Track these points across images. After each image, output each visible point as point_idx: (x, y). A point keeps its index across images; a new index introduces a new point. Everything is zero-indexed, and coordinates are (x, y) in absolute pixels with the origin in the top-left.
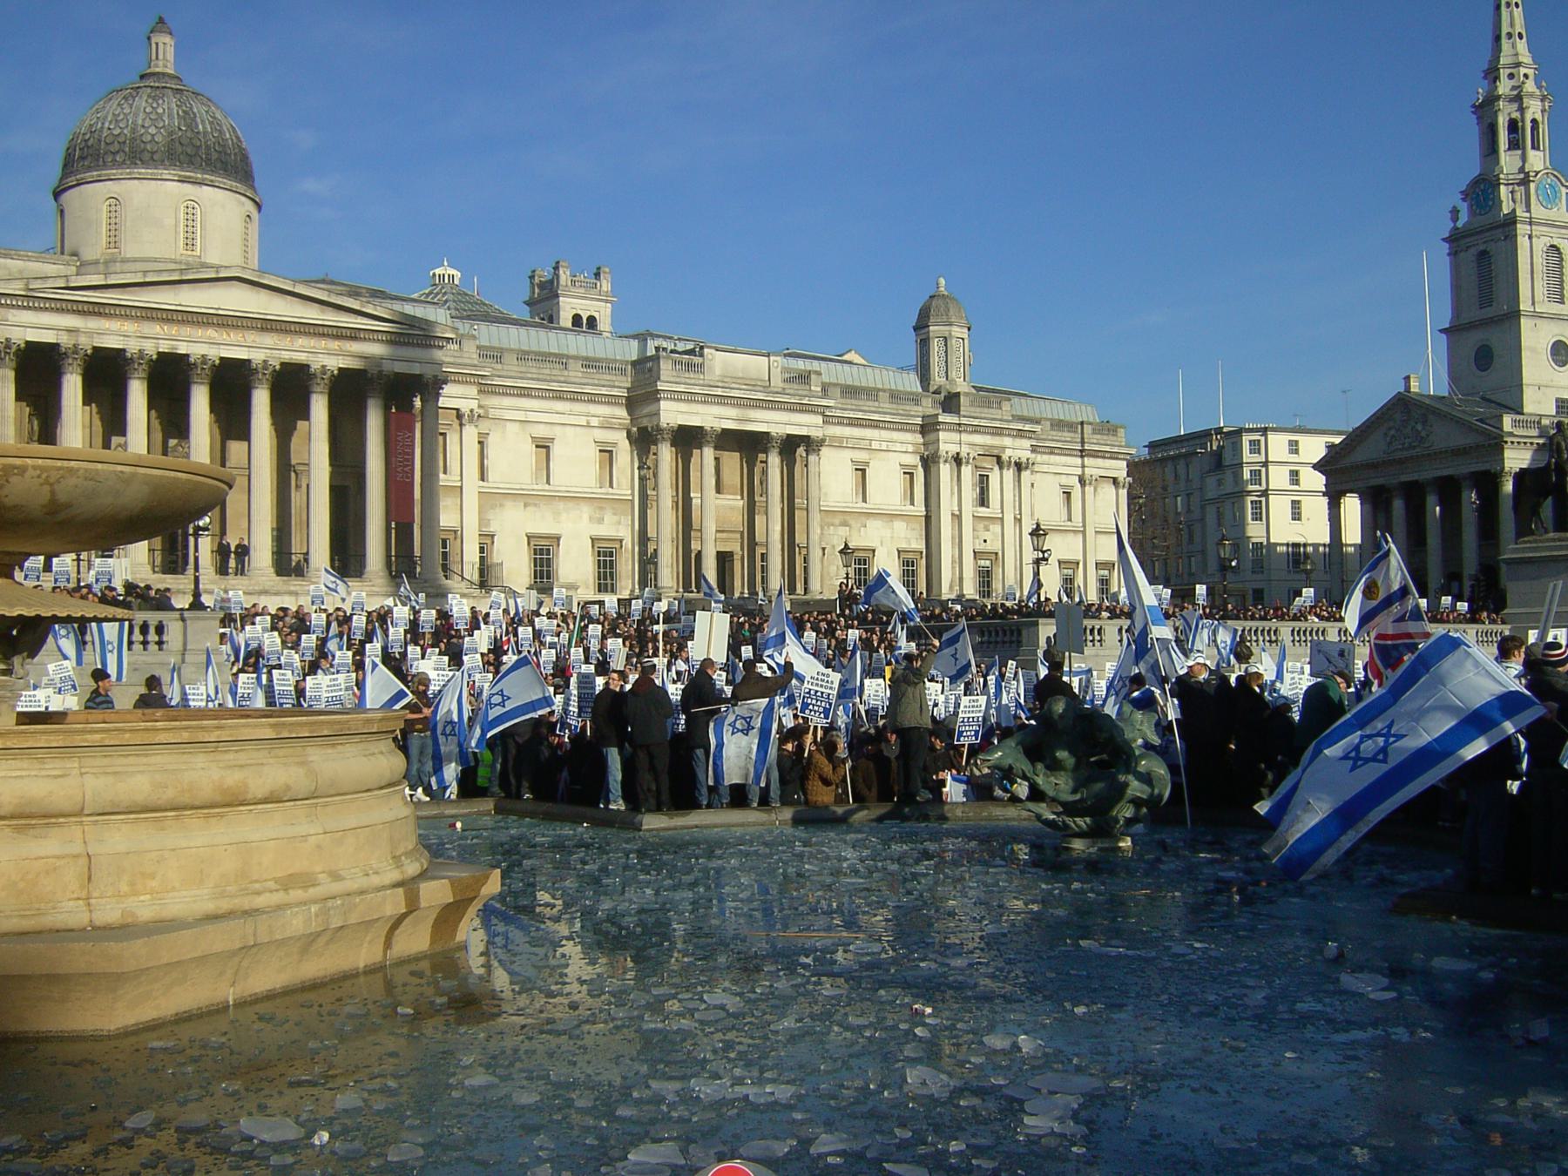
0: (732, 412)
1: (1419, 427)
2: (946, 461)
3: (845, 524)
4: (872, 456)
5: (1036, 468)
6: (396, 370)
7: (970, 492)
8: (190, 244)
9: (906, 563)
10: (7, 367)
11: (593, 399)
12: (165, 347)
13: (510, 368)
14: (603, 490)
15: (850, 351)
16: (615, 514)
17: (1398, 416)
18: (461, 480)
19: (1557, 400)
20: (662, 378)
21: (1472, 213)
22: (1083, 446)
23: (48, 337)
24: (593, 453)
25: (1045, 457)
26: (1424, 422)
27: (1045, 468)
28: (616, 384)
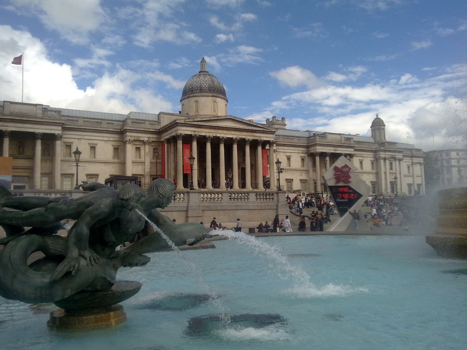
0: (333, 148)
2: (382, 159)
6: (264, 140)
7: (388, 167)
8: (214, 111)
11: (299, 146)
12: (214, 135)
23: (189, 133)
24: (300, 159)
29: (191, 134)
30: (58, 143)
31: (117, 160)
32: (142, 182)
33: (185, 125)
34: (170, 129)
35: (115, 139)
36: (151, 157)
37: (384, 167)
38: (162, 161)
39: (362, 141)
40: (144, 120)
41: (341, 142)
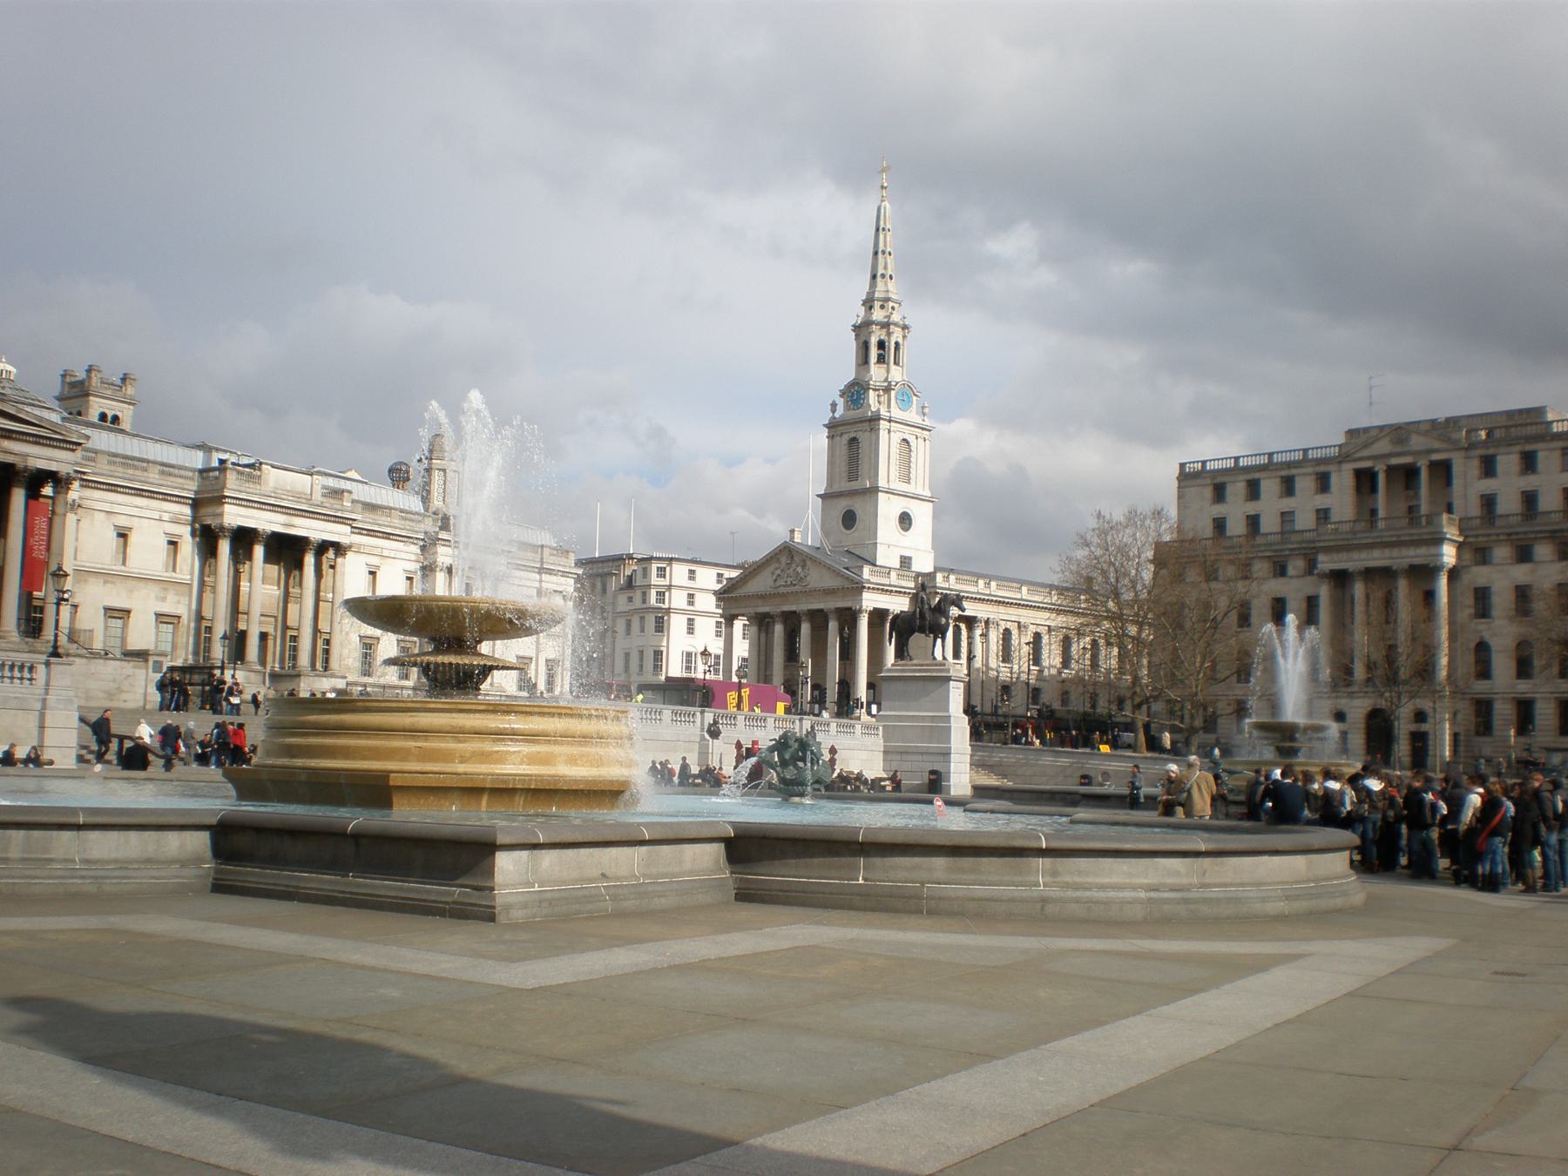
0: (282, 518)
1: (799, 569)
2: (441, 570)
4: (382, 562)
6: (39, 467)
11: (166, 497)
15: (351, 470)
16: (175, 594)
17: (784, 560)
19: (901, 557)
20: (227, 486)
21: (847, 408)
22: (542, 564)
24: (162, 543)
26: (803, 567)
28: (186, 487)
39: (385, 504)
41: (311, 499)
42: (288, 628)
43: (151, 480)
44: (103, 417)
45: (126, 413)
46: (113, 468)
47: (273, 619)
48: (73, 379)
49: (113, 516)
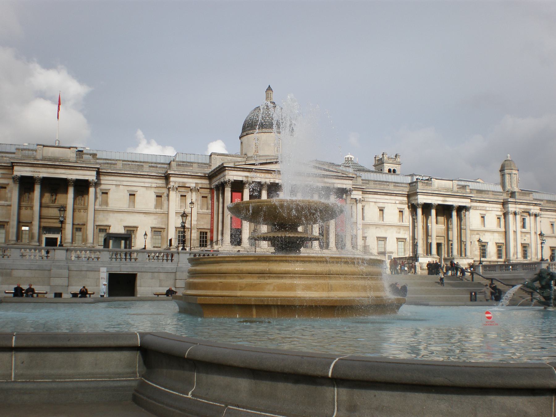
0: (441, 198)
2: (511, 214)
3: (478, 234)
5: (542, 216)
6: (339, 187)
7: (519, 224)
9: (499, 247)
10: (228, 187)
11: (396, 195)
12: (272, 181)
13: (371, 185)
14: (400, 223)
15: (478, 179)
16: (404, 231)
18: (357, 220)
20: (419, 188)
23: (240, 179)
25: (545, 213)
27: (545, 216)
28: (404, 190)
29: (242, 180)
30: (92, 190)
31: (160, 210)
32: (186, 237)
33: (235, 168)
34: (220, 174)
35: (158, 185)
36: (199, 206)
37: (514, 224)
38: (211, 212)
39: (486, 189)
40: (192, 163)
42: (449, 241)
43: (391, 189)
44: (390, 171)
45: (397, 168)
46: (375, 186)
47: (443, 238)
48: (379, 158)
49: (377, 203)
